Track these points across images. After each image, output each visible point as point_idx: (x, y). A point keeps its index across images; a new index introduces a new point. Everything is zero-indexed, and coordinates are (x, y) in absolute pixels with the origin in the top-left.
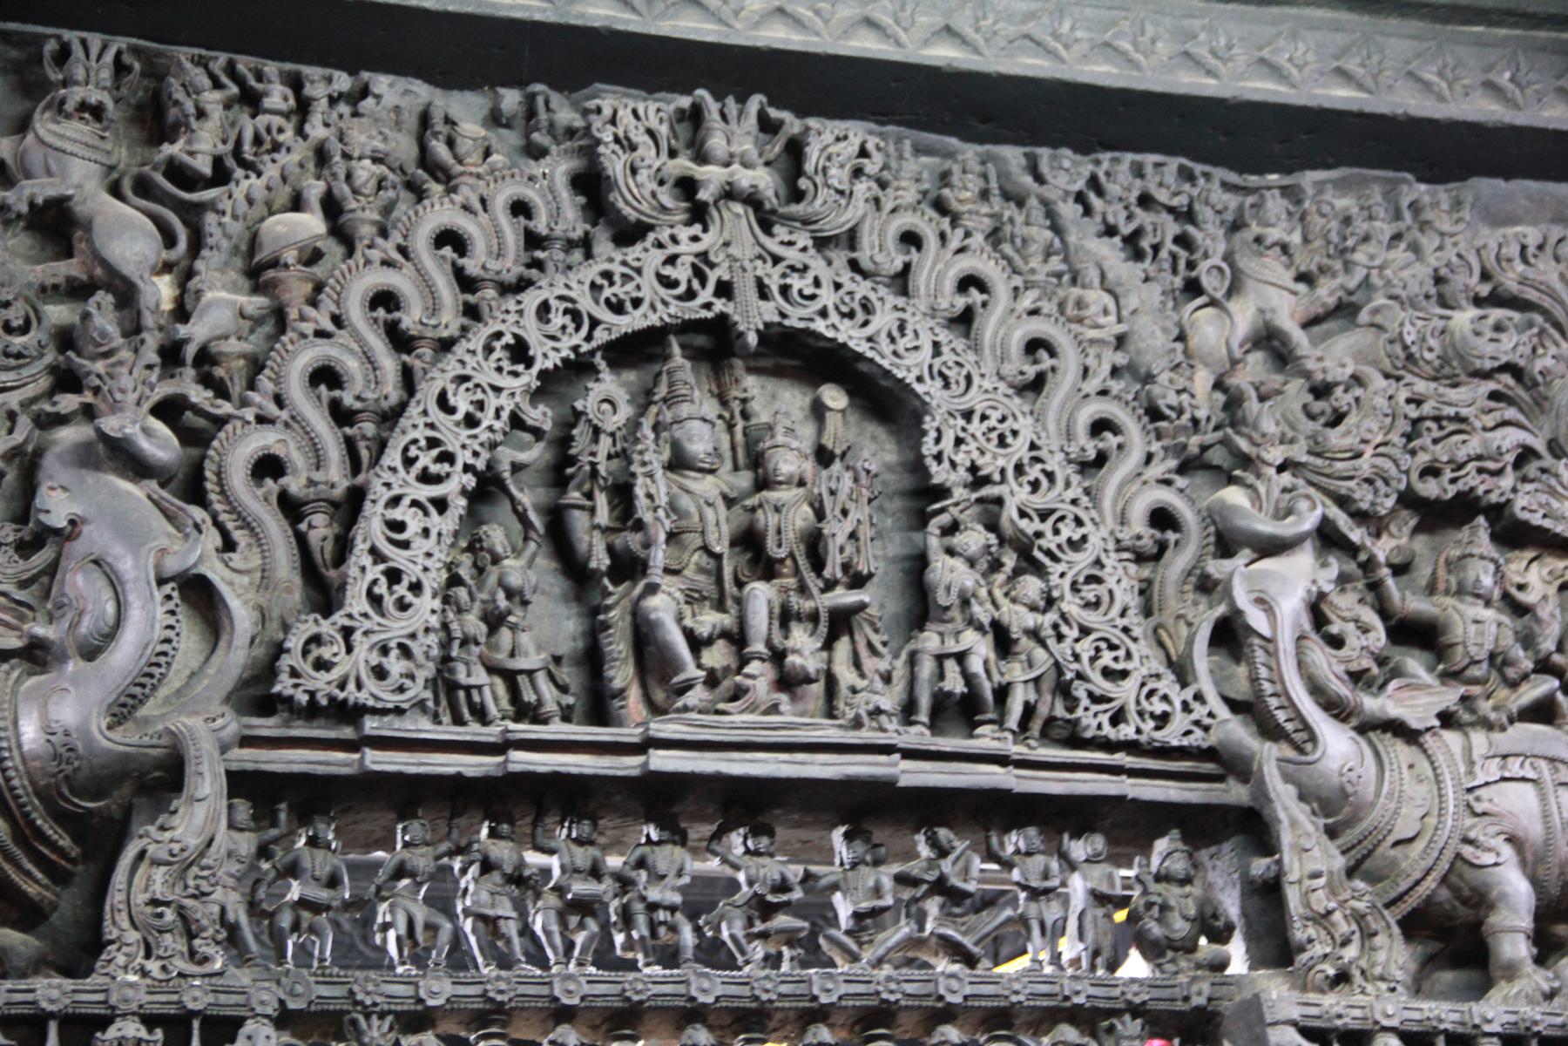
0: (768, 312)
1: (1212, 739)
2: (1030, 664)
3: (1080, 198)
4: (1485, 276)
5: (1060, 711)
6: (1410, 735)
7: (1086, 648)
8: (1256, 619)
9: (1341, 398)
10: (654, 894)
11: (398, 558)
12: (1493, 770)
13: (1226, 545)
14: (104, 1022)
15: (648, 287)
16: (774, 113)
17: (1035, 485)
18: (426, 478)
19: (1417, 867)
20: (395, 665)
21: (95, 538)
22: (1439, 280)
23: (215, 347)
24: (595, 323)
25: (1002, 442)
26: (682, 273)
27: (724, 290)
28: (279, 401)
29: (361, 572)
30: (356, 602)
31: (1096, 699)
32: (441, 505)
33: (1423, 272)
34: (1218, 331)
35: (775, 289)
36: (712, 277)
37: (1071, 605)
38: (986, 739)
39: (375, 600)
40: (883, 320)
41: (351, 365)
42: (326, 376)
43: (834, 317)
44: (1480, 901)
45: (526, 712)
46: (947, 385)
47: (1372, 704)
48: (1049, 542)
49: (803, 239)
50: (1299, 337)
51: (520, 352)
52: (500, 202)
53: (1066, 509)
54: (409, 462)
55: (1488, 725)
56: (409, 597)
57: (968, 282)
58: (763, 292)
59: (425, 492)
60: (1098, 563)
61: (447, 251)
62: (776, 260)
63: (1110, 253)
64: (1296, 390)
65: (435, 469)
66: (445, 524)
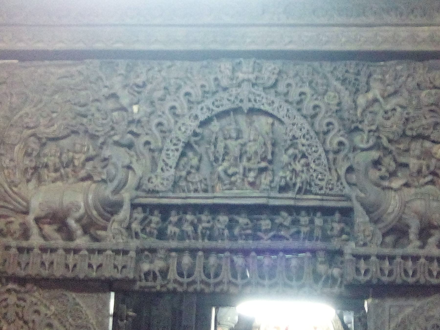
0: (250, 105)
1: (343, 193)
2: (302, 177)
3: (332, 72)
4: (431, 83)
5: (308, 188)
6: (396, 190)
7: (315, 175)
8: (355, 166)
9: (390, 114)
10: (219, 226)
11: (167, 161)
12: (414, 197)
13: (355, 149)
14: (105, 250)
15: (225, 102)
16: (258, 61)
17: (307, 140)
18: (175, 145)
19: (390, 219)
20: (165, 182)
21: (114, 160)
22: (418, 85)
23: (142, 120)
24: (212, 110)
25: (301, 130)
26: (232, 98)
27: (241, 101)
28: (150, 130)
29: (161, 164)
30: (159, 170)
31: (316, 185)
32: (177, 150)
33: (415, 83)
34: (362, 100)
35: (253, 100)
36: (239, 98)
37: (313, 165)
38: (290, 194)
39: (162, 169)
40: (276, 105)
41: (165, 122)
42: (160, 124)
43: (266, 105)
44: (408, 226)
45: (196, 191)
46: (289, 117)
47: (386, 183)
48: (309, 151)
49: (261, 89)
50: (381, 100)
51: (196, 117)
52: (199, 85)
53: (314, 144)
54: (171, 141)
55: (416, 187)
56: (169, 169)
57: (302, 94)
58: (250, 100)
59: (173, 148)
60: (320, 155)
61: (187, 97)
62: (254, 93)
63: (338, 84)
64: (381, 113)
65: (176, 142)
66: (177, 154)
